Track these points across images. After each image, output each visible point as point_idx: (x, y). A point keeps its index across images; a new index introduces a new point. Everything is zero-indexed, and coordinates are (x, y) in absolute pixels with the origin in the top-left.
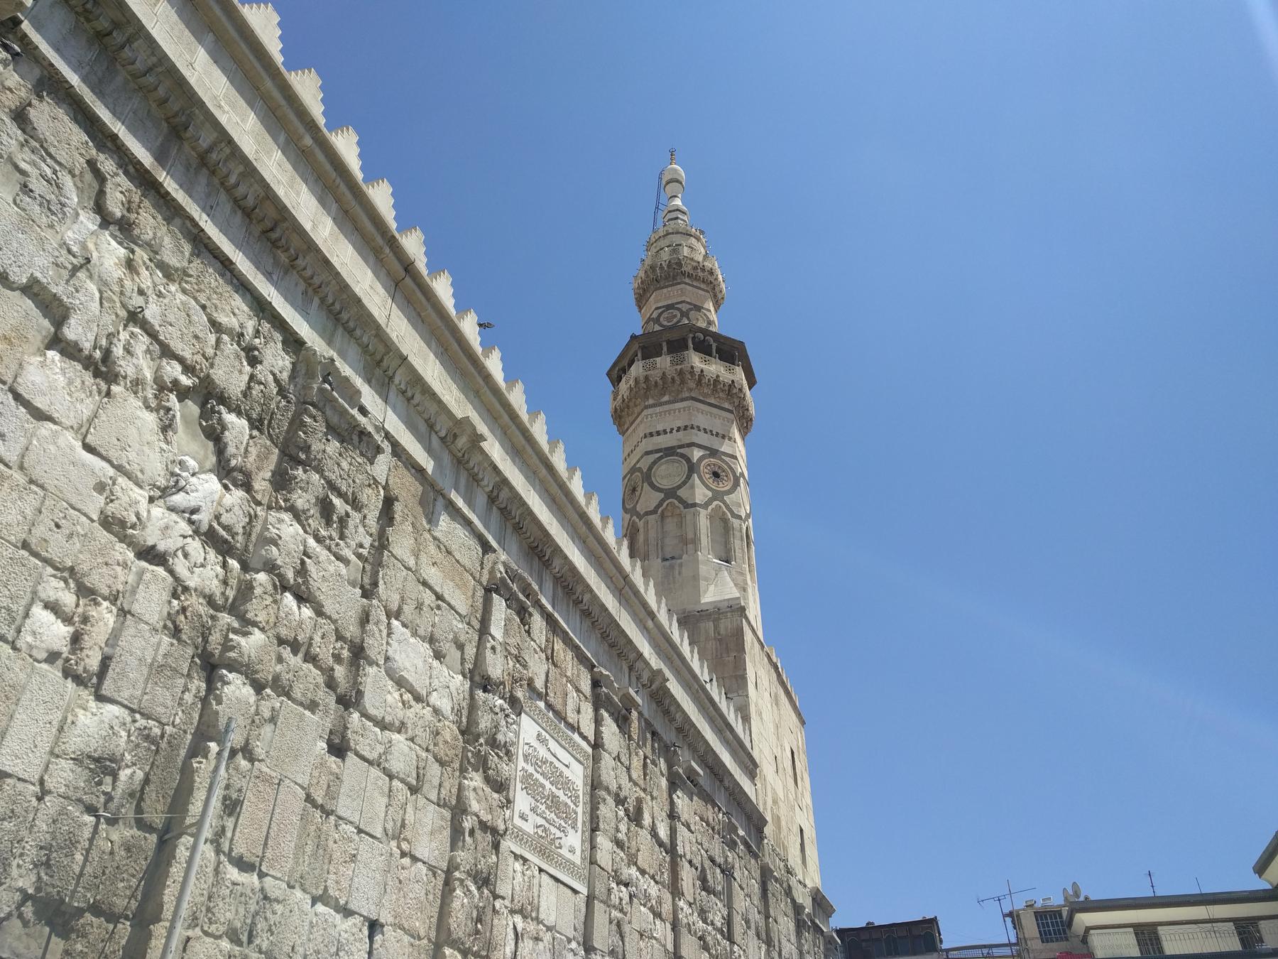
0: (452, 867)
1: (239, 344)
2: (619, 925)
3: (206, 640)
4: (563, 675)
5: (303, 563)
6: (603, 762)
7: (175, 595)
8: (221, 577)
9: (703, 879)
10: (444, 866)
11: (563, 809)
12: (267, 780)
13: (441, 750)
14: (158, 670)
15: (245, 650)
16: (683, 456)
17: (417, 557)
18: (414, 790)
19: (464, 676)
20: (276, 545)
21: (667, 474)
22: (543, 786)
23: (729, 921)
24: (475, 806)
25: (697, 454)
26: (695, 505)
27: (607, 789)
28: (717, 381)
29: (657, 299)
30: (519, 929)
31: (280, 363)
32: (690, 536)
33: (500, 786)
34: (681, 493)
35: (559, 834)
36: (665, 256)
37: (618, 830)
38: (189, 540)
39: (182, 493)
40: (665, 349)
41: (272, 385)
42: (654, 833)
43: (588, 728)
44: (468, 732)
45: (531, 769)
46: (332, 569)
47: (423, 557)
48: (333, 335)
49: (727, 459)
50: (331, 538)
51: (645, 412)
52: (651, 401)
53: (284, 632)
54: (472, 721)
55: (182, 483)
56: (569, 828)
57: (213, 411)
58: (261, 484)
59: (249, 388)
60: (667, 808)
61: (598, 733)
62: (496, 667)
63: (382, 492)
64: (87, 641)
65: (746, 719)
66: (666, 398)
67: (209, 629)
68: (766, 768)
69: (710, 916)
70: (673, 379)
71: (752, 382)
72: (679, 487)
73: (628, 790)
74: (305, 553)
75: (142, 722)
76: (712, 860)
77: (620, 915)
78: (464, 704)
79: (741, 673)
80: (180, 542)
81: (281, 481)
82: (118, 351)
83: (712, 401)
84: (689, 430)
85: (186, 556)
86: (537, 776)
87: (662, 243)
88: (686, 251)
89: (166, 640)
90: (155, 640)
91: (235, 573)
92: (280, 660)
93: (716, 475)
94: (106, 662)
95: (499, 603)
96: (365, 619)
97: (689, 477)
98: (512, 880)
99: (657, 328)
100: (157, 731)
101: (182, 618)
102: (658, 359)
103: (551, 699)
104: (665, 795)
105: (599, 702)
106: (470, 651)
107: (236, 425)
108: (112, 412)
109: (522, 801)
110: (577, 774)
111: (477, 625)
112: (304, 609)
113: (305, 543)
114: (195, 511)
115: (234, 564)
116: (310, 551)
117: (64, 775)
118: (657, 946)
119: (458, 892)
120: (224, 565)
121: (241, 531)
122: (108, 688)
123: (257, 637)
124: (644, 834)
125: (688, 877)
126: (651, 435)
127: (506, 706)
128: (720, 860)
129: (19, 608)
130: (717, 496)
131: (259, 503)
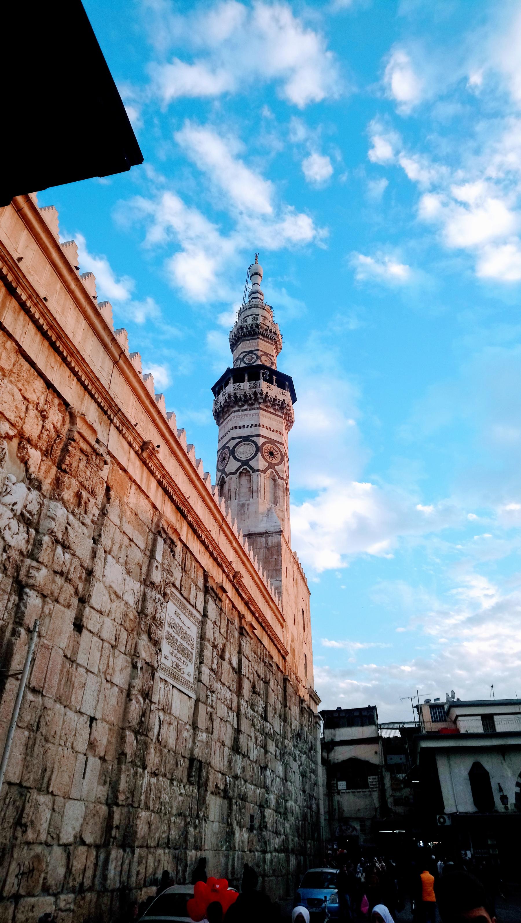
0: (130, 686)
1: (37, 409)
2: (211, 715)
3: (18, 574)
4: (189, 577)
5: (66, 528)
6: (207, 625)
7: (4, 551)
8: (26, 539)
9: (254, 687)
10: (126, 687)
11: (186, 651)
12: (47, 648)
13: (127, 624)
16: (253, 442)
17: (121, 519)
18: (114, 647)
19: (140, 582)
20: (54, 519)
21: (244, 451)
22: (177, 640)
23: (266, 710)
24: (143, 655)
25: (260, 441)
27: (209, 640)
28: (275, 400)
29: (245, 346)
30: (162, 719)
31: (57, 418)
32: (255, 488)
33: (156, 643)
34: (250, 463)
35: (183, 666)
36: (249, 321)
37: (212, 662)
38: (12, 520)
39: (9, 495)
40: (246, 378)
41: (53, 431)
42: (230, 663)
43: (200, 607)
44: (142, 613)
45: (171, 631)
46: (80, 531)
47: (124, 519)
48: (83, 399)
49: (278, 445)
50: (80, 514)
51: (233, 414)
52: (237, 408)
53: (57, 568)
54: (144, 608)
55: (9, 490)
56: (188, 662)
57: (24, 448)
58: (47, 486)
59: (41, 432)
60: (237, 648)
61: (205, 609)
62: (157, 577)
63: (105, 484)
65: (280, 594)
66: (246, 407)
67: (20, 567)
68: (289, 621)
69: (256, 708)
70: (250, 395)
71: (294, 399)
72: (250, 460)
73: (220, 641)
74: (68, 523)
76: (259, 676)
77: (211, 710)
78: (141, 599)
79: (279, 567)
81: (58, 483)
83: (272, 411)
84: (258, 427)
85: (10, 529)
86: (174, 634)
87: (248, 312)
88: (261, 320)
91: (33, 536)
92: (54, 581)
93: (271, 454)
95: (160, 541)
96: (94, 555)
97: (256, 454)
98: (160, 693)
99: (243, 365)
101: (7, 563)
102: (242, 384)
103: (182, 592)
104: (237, 641)
105: (207, 590)
106: (144, 568)
107: (35, 456)
109: (166, 647)
110: (193, 632)
111: (148, 553)
112: (66, 554)
113: (67, 518)
114: (15, 504)
115: (32, 531)
116: (70, 522)
118: (228, 725)
119: (134, 701)
120: (28, 532)
121: (36, 513)
123: (44, 571)
124: (225, 664)
125: (246, 686)
126: (236, 428)
127: (161, 598)
128: (262, 676)
130: (272, 466)
131: (45, 497)
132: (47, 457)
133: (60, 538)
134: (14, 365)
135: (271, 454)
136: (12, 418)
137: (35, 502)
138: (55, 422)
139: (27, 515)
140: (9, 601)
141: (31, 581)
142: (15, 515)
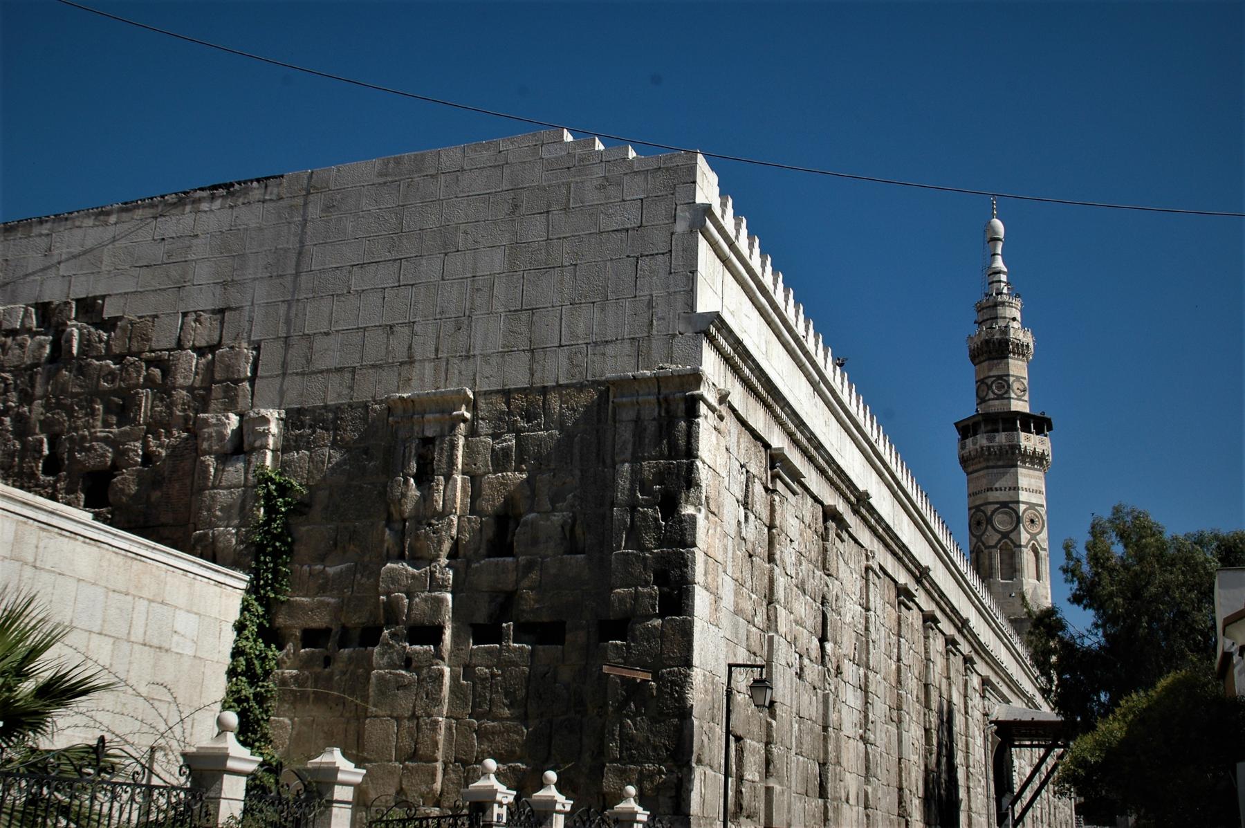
26: (1020, 546)
28: (1034, 452)
34: (1012, 536)
93: (1032, 521)
130: (1033, 537)
135: (1032, 521)
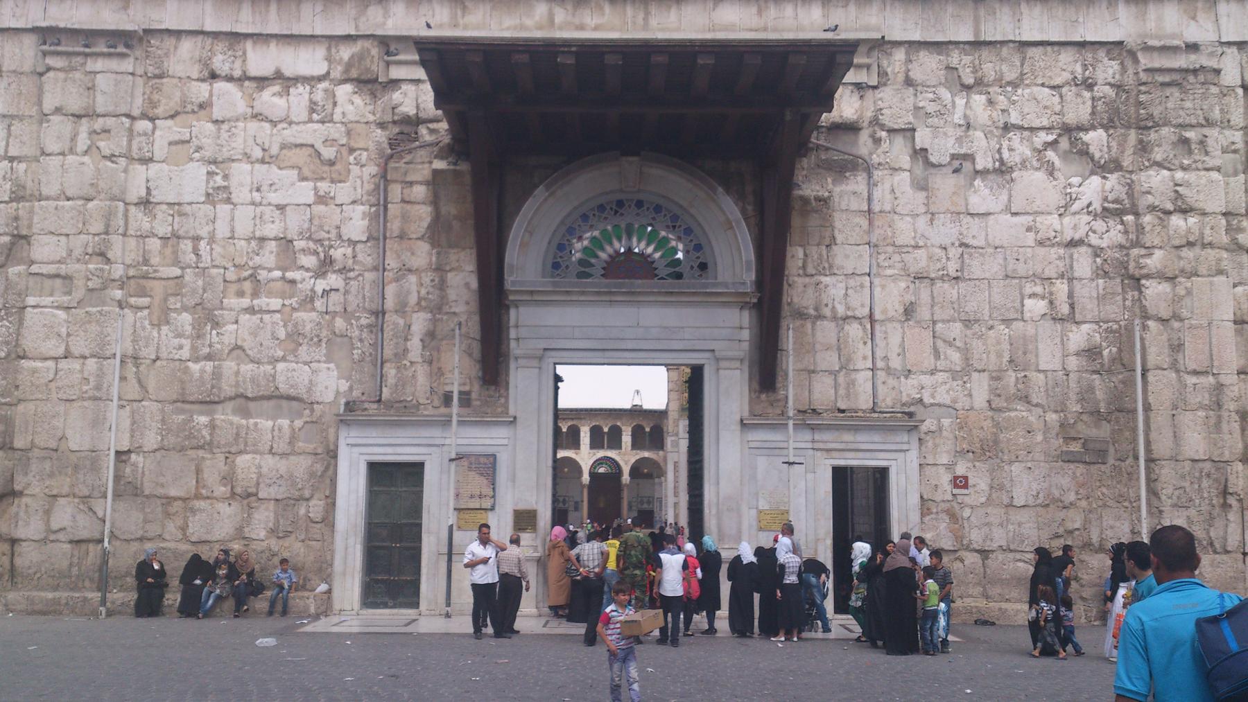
5: (1176, 192)
14: (1101, 299)
15: (1152, 266)
31: (1111, 71)
53: (1177, 242)
59: (1094, 107)
64: (1057, 303)
74: (1176, 185)
75: (1105, 326)
80: (1087, 228)
81: (1143, 148)
82: (1006, 154)
85: (1094, 232)
89: (1101, 281)
90: (1094, 284)
92: (1180, 258)
94: (1072, 306)
100: (1115, 327)
107: (1096, 139)
108: (1017, 188)
114: (1089, 205)
117: (1073, 363)
120: (1122, 223)
121: (1125, 197)
122: (1078, 317)
123: (1158, 254)
129: (1018, 304)
132: (1114, 127)
133: (1170, 207)
134: (1022, 65)
136: (1045, 123)
137: (1117, 187)
138: (1111, 80)
139: (1111, 206)
140: (1125, 300)
141: (1145, 271)
142: (1096, 215)
